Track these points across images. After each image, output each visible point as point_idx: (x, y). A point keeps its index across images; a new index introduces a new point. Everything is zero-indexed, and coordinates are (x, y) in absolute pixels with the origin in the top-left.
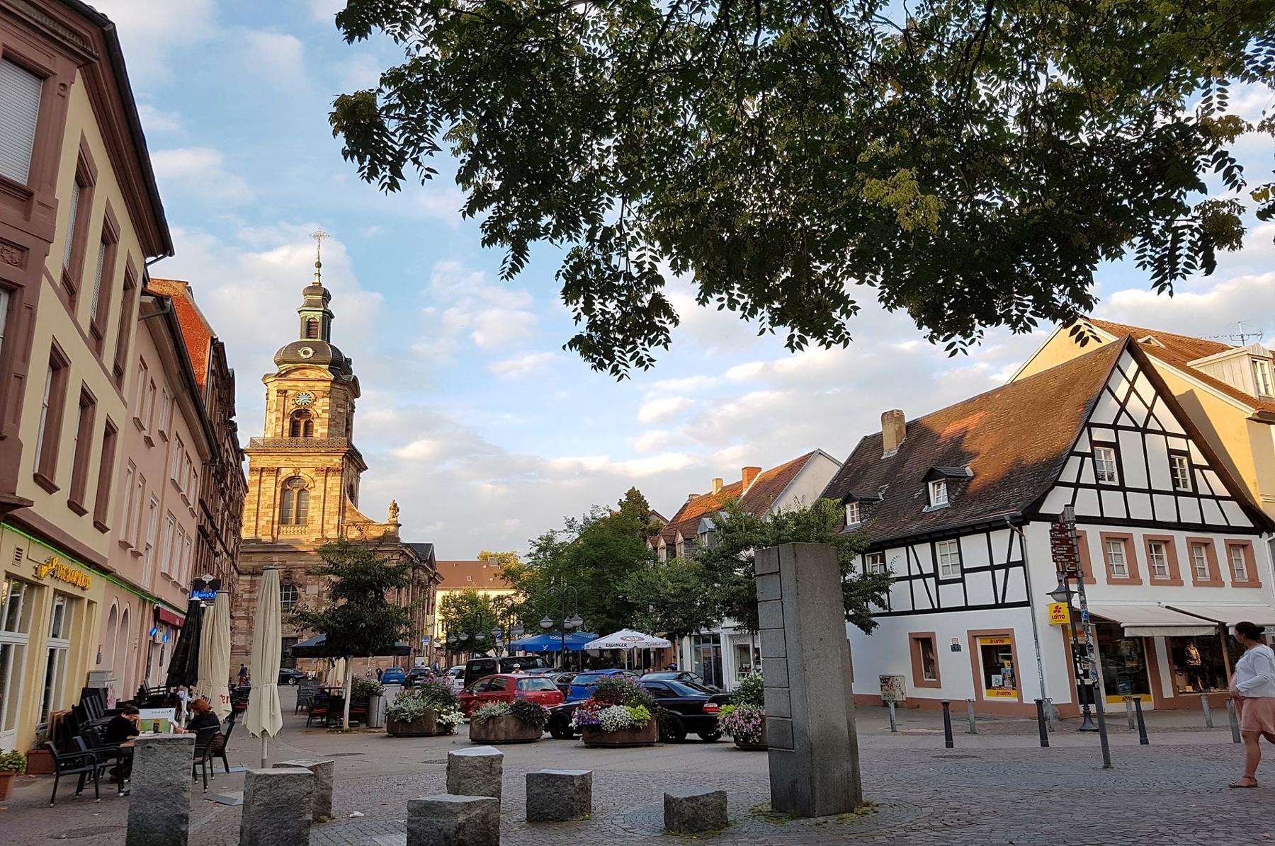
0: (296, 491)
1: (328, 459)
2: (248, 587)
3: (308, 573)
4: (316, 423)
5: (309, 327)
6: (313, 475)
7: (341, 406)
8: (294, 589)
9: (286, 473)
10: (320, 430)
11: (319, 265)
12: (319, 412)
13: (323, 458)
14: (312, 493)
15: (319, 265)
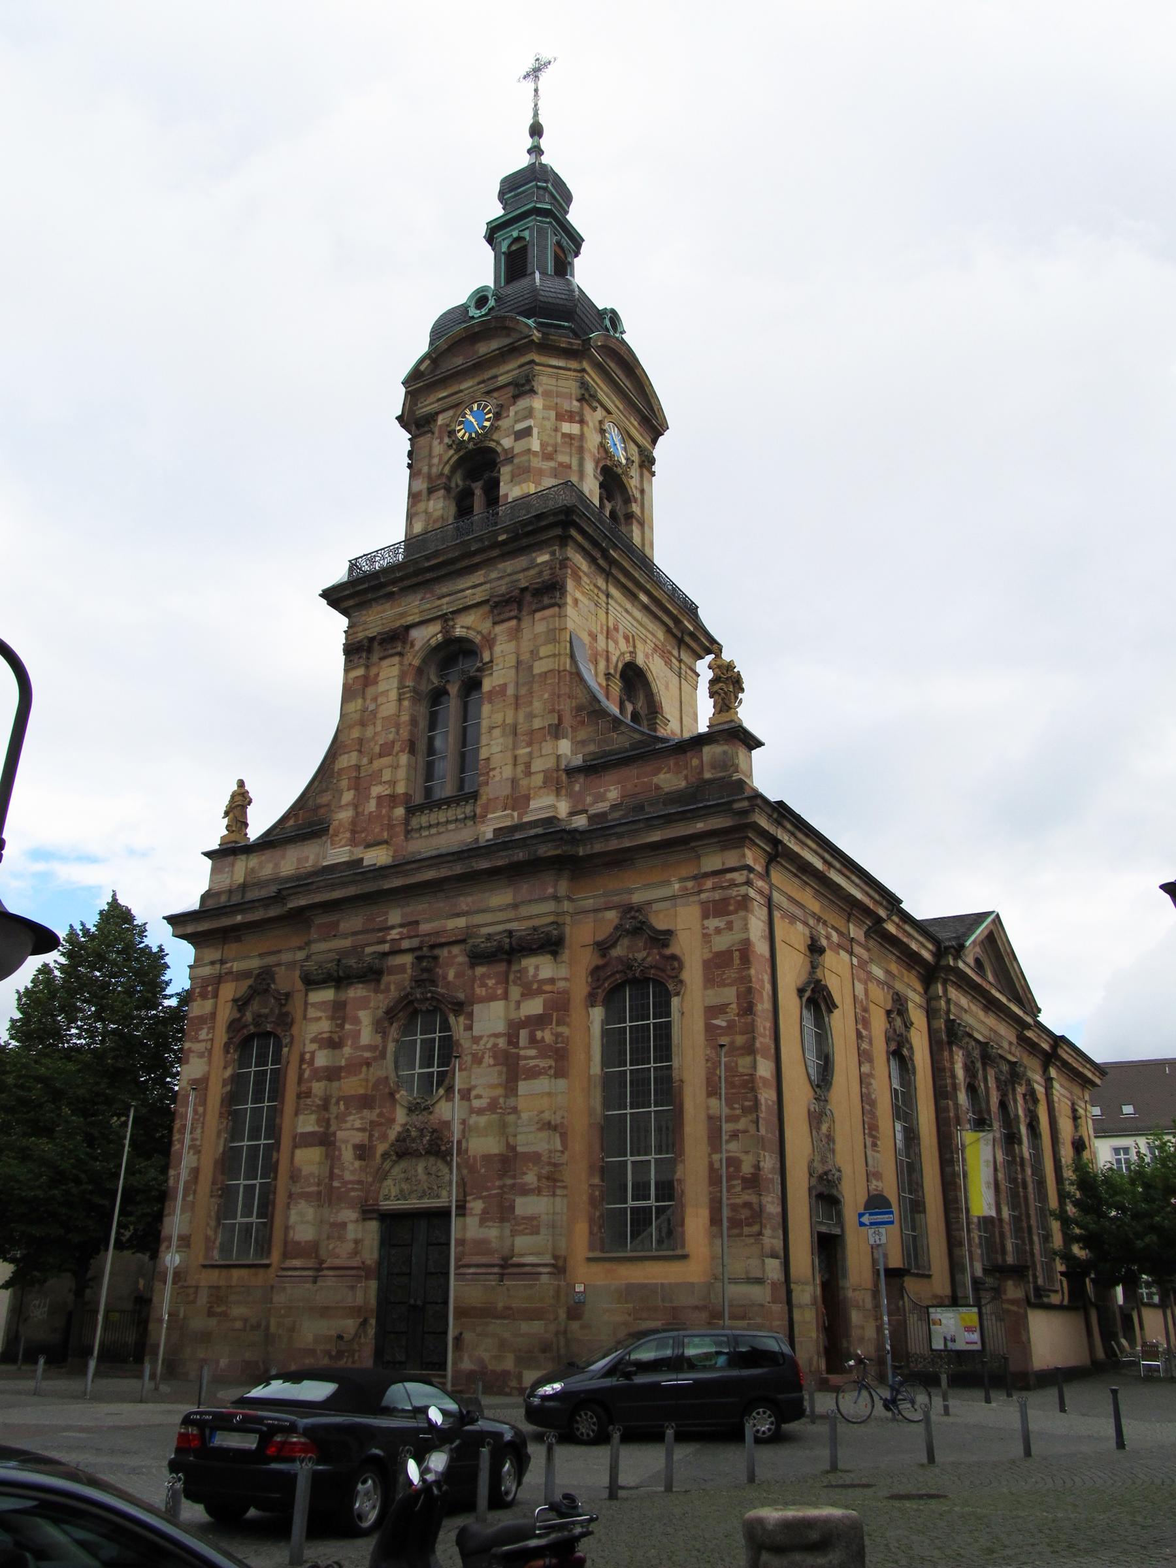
0: (453, 689)
1: (521, 562)
2: (324, 1026)
3: (477, 957)
4: (505, 471)
5: (513, 264)
6: (486, 626)
7: (570, 417)
8: (446, 1027)
9: (426, 636)
10: (511, 490)
11: (536, 130)
12: (507, 442)
13: (509, 566)
14: (487, 685)
15: (536, 130)
